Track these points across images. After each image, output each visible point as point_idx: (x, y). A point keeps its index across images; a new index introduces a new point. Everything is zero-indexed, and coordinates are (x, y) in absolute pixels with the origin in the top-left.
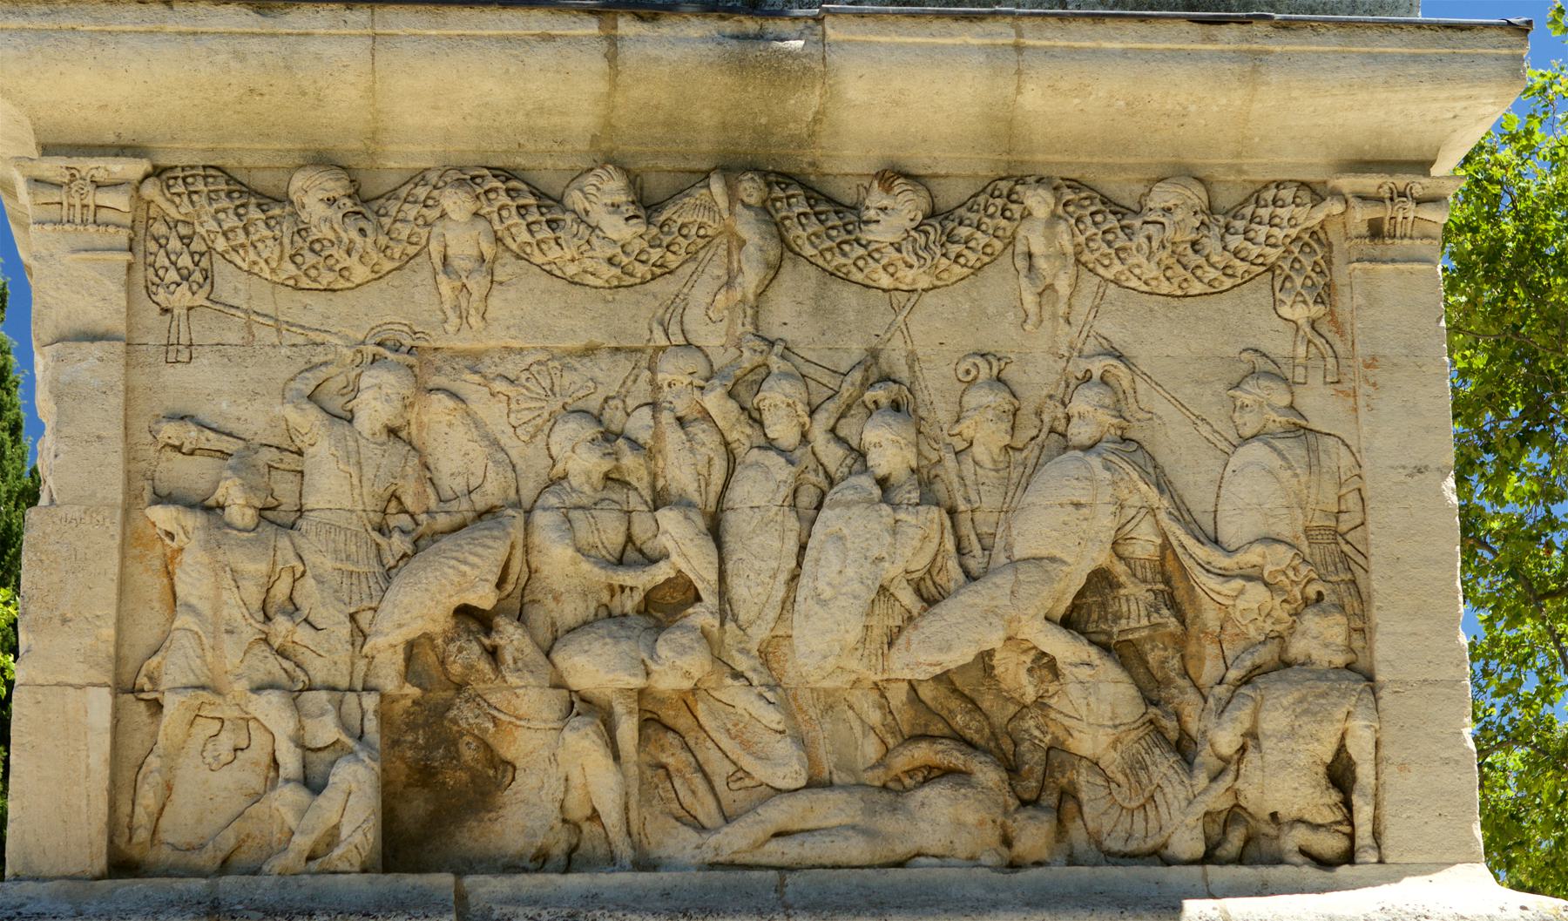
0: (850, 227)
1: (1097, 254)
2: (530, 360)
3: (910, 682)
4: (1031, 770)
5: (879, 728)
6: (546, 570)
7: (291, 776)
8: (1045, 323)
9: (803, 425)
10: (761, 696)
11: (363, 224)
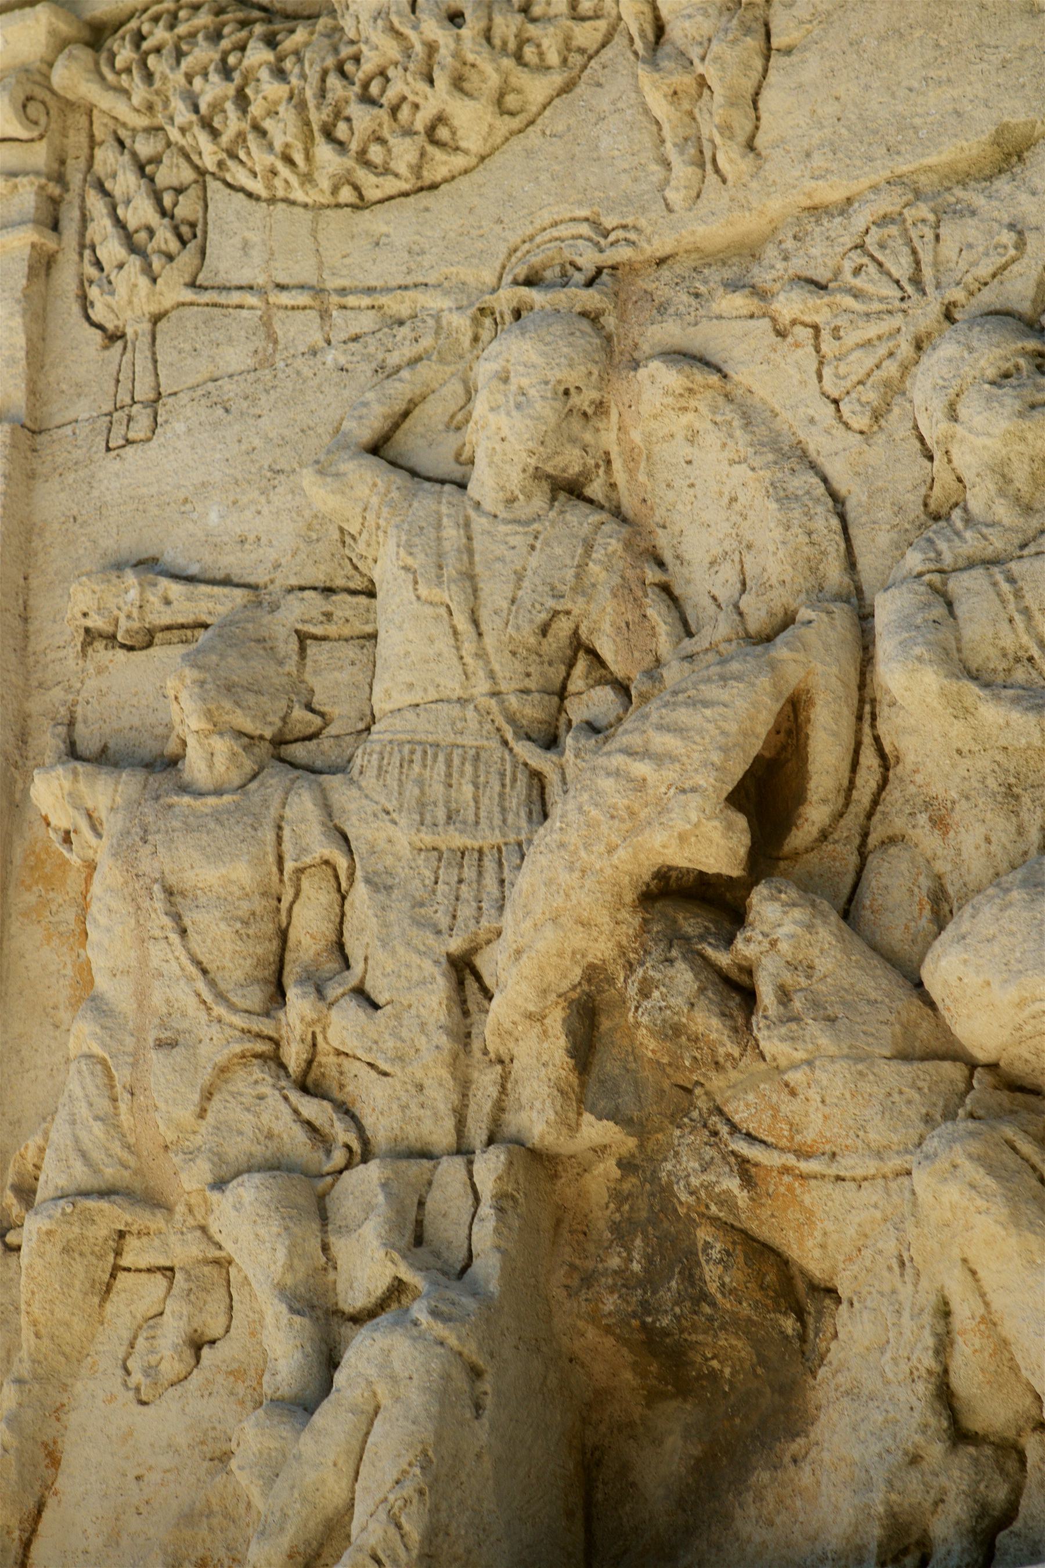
2: (861, 218)
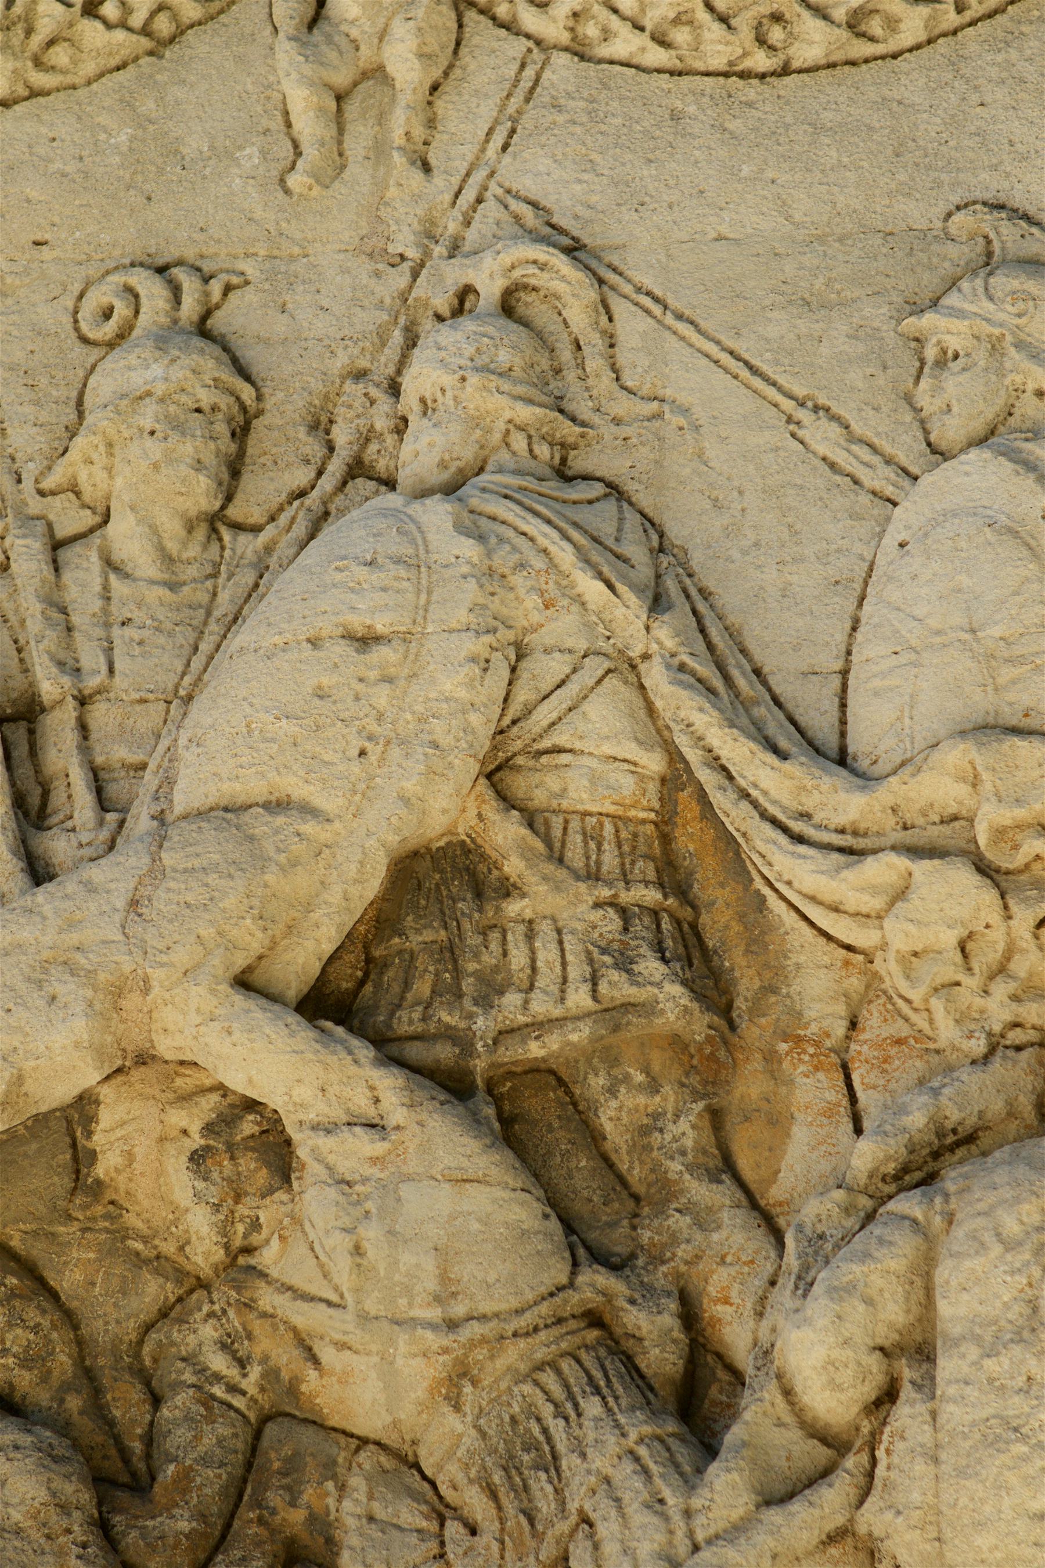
4: (186, 1476)
8: (353, 170)
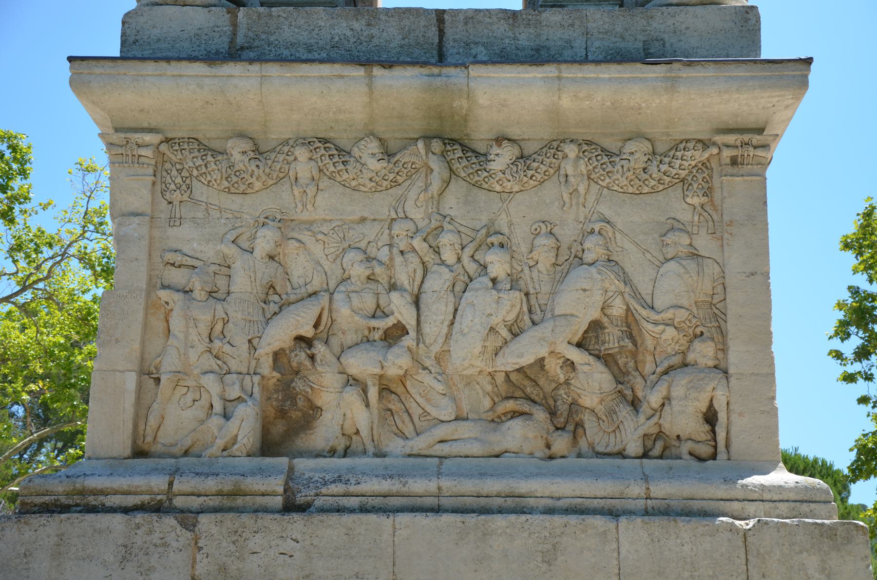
0: (482, 163)
1: (598, 175)
2: (334, 225)
3: (506, 372)
4: (561, 414)
5: (491, 393)
6: (339, 320)
7: (218, 412)
8: (573, 207)
9: (459, 254)
10: (435, 378)
11: (258, 163)
